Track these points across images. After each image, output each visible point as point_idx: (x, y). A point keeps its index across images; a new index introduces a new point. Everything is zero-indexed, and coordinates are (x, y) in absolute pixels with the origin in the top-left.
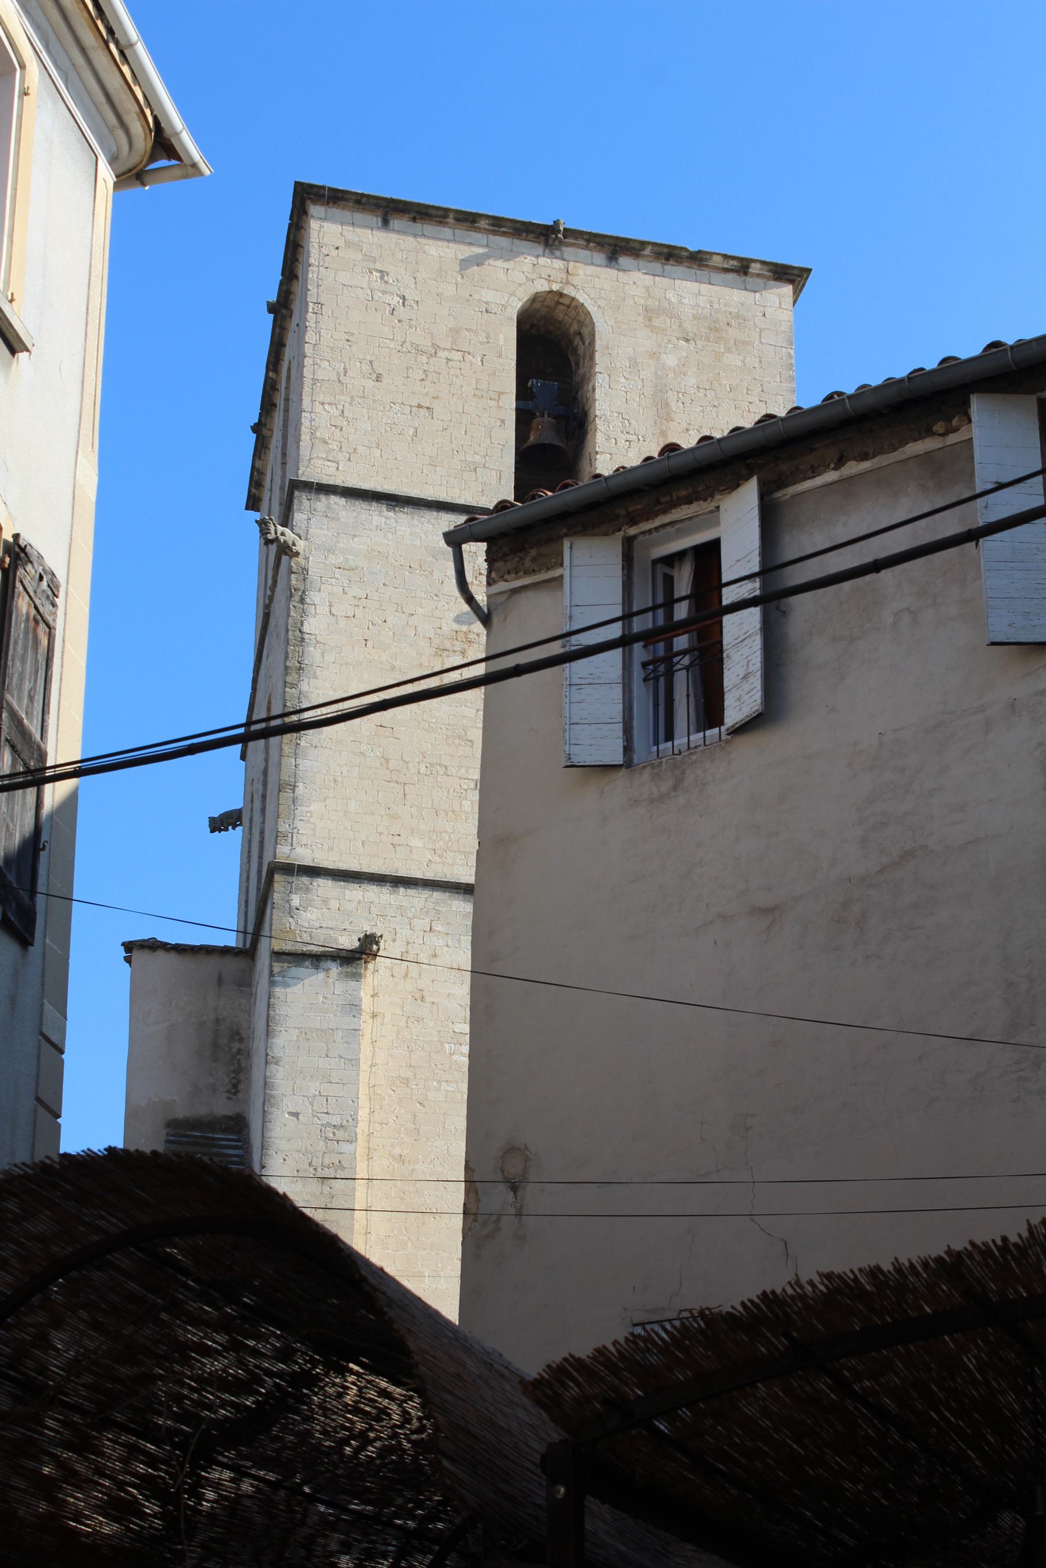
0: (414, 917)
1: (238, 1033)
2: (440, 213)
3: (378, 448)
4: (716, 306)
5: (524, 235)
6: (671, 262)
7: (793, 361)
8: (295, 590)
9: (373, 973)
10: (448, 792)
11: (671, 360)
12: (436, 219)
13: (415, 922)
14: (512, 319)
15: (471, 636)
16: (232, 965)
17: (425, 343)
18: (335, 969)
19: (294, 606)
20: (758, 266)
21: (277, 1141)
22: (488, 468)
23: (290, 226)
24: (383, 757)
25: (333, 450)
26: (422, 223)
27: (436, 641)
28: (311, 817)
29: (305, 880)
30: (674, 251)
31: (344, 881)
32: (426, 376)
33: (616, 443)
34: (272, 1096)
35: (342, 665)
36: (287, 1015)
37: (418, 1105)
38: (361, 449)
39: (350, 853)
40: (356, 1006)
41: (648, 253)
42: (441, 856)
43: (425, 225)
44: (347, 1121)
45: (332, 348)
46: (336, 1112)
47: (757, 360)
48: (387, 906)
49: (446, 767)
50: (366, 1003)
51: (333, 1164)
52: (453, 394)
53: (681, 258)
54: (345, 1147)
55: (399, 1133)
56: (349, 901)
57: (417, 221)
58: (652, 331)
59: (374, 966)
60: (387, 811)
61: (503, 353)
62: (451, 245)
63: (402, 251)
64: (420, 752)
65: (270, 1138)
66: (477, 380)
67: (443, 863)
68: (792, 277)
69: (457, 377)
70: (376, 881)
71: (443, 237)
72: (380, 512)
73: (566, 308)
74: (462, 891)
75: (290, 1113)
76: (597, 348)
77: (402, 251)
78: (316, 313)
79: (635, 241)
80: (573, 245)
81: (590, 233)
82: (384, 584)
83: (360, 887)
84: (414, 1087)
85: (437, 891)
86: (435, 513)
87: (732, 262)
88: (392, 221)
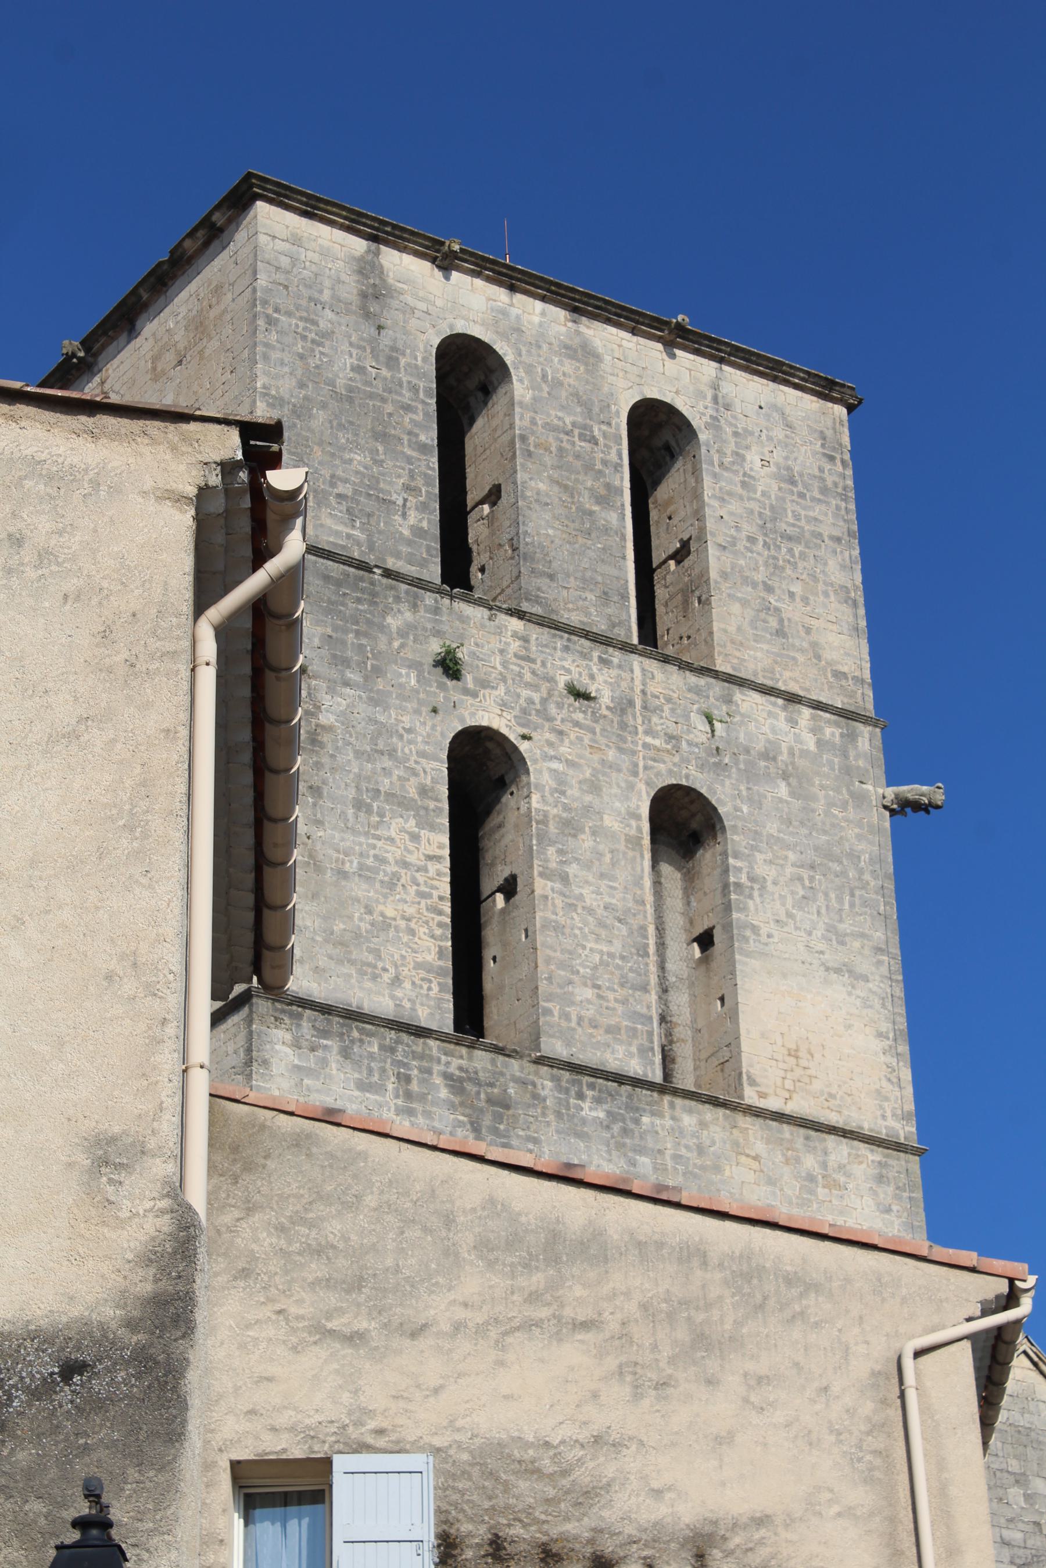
6: (170, 283)
79: (127, 297)
81: (98, 327)
87: (200, 234)
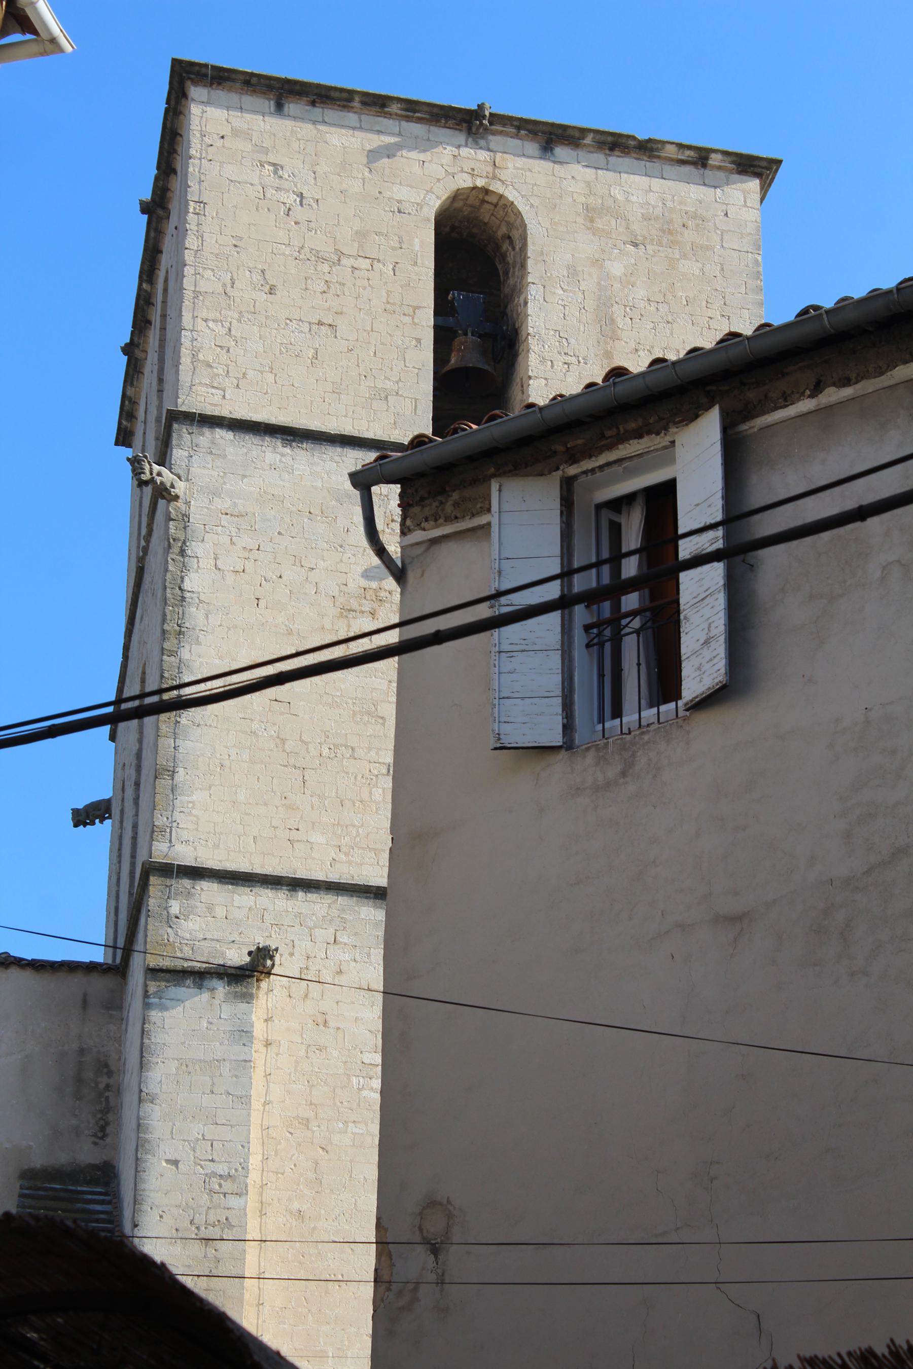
0: (316, 927)
1: (106, 1065)
2: (344, 95)
3: (271, 372)
4: (669, 204)
5: (443, 121)
6: (617, 153)
7: (761, 269)
8: (174, 540)
9: (267, 994)
10: (355, 778)
11: (617, 268)
12: (338, 103)
13: (318, 932)
14: (429, 220)
15: (382, 594)
16: (99, 984)
17: (327, 249)
18: (221, 988)
19: (173, 560)
20: (719, 157)
21: (152, 1195)
22: (402, 396)
23: (167, 111)
24: (278, 737)
25: (218, 375)
26: (322, 108)
27: (341, 600)
28: (193, 808)
29: (186, 882)
30: (620, 140)
31: (232, 884)
32: (328, 287)
33: (552, 367)
34: (147, 1141)
35: (229, 629)
36: (164, 1044)
37: (321, 1151)
38: (251, 374)
39: (240, 851)
40: (247, 1032)
41: (589, 142)
42: (346, 854)
43: (325, 110)
44: (236, 1170)
45: (217, 256)
46: (223, 1159)
47: (719, 268)
48: (284, 914)
49: (353, 749)
50: (259, 1029)
51: (219, 1221)
52: (360, 309)
53: (627, 148)
54: (233, 1201)
55: (298, 1185)
56: (239, 907)
57: (317, 105)
58: (594, 234)
59: (269, 985)
60: (284, 801)
61: (419, 261)
62: (357, 133)
63: (299, 140)
64: (322, 731)
65: (144, 1190)
66: (389, 293)
67: (350, 863)
68: (756, 170)
69: (365, 288)
70: (271, 884)
71: (347, 124)
72: (274, 448)
73: (492, 207)
74: (372, 896)
75: (168, 1161)
76: (529, 254)
77: (299, 140)
78: (198, 214)
79: (574, 128)
80: (501, 133)
81: (521, 119)
82: (279, 533)
83: (251, 891)
84: (315, 1129)
85: (342, 895)
86: (339, 450)
88: (286, 106)
